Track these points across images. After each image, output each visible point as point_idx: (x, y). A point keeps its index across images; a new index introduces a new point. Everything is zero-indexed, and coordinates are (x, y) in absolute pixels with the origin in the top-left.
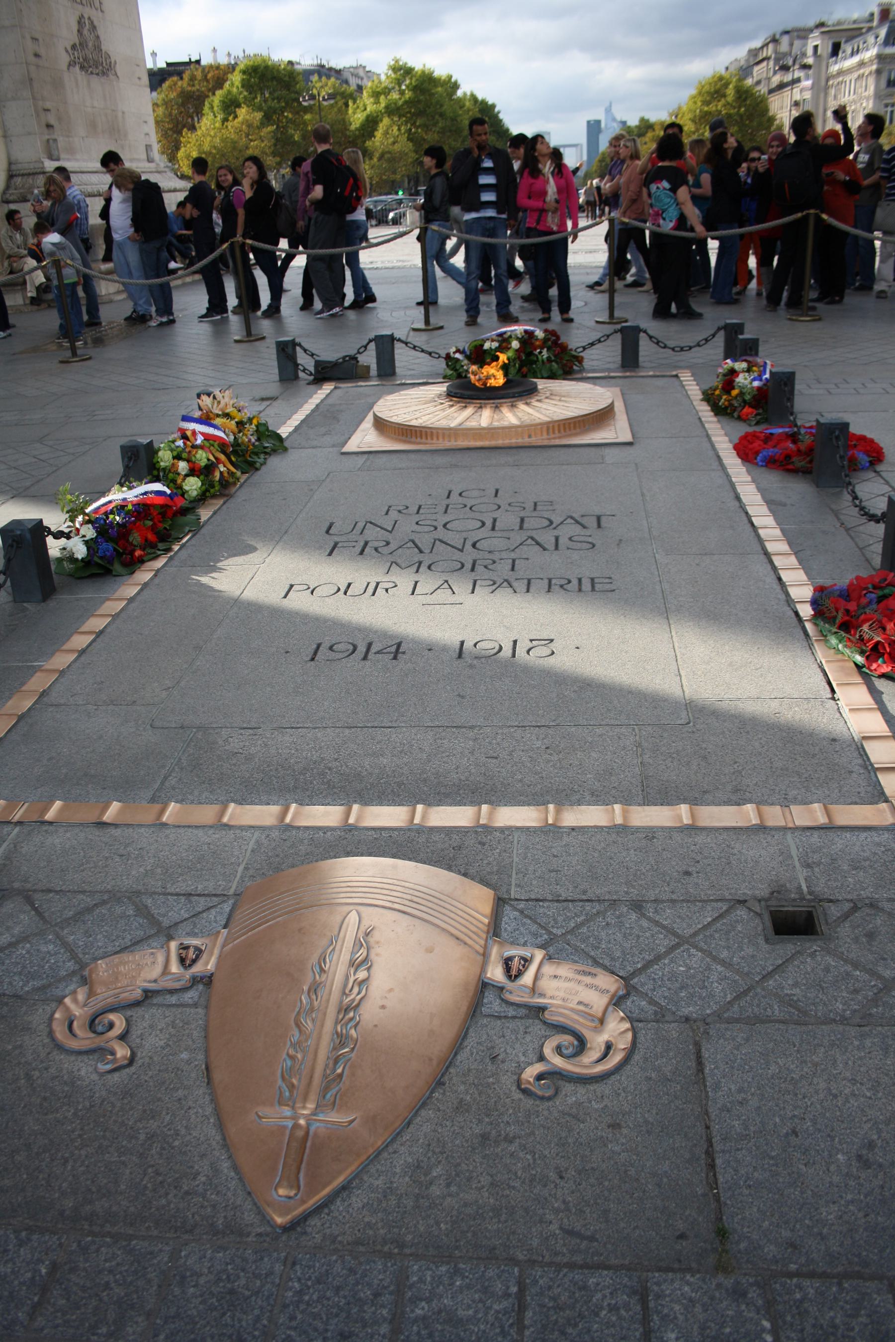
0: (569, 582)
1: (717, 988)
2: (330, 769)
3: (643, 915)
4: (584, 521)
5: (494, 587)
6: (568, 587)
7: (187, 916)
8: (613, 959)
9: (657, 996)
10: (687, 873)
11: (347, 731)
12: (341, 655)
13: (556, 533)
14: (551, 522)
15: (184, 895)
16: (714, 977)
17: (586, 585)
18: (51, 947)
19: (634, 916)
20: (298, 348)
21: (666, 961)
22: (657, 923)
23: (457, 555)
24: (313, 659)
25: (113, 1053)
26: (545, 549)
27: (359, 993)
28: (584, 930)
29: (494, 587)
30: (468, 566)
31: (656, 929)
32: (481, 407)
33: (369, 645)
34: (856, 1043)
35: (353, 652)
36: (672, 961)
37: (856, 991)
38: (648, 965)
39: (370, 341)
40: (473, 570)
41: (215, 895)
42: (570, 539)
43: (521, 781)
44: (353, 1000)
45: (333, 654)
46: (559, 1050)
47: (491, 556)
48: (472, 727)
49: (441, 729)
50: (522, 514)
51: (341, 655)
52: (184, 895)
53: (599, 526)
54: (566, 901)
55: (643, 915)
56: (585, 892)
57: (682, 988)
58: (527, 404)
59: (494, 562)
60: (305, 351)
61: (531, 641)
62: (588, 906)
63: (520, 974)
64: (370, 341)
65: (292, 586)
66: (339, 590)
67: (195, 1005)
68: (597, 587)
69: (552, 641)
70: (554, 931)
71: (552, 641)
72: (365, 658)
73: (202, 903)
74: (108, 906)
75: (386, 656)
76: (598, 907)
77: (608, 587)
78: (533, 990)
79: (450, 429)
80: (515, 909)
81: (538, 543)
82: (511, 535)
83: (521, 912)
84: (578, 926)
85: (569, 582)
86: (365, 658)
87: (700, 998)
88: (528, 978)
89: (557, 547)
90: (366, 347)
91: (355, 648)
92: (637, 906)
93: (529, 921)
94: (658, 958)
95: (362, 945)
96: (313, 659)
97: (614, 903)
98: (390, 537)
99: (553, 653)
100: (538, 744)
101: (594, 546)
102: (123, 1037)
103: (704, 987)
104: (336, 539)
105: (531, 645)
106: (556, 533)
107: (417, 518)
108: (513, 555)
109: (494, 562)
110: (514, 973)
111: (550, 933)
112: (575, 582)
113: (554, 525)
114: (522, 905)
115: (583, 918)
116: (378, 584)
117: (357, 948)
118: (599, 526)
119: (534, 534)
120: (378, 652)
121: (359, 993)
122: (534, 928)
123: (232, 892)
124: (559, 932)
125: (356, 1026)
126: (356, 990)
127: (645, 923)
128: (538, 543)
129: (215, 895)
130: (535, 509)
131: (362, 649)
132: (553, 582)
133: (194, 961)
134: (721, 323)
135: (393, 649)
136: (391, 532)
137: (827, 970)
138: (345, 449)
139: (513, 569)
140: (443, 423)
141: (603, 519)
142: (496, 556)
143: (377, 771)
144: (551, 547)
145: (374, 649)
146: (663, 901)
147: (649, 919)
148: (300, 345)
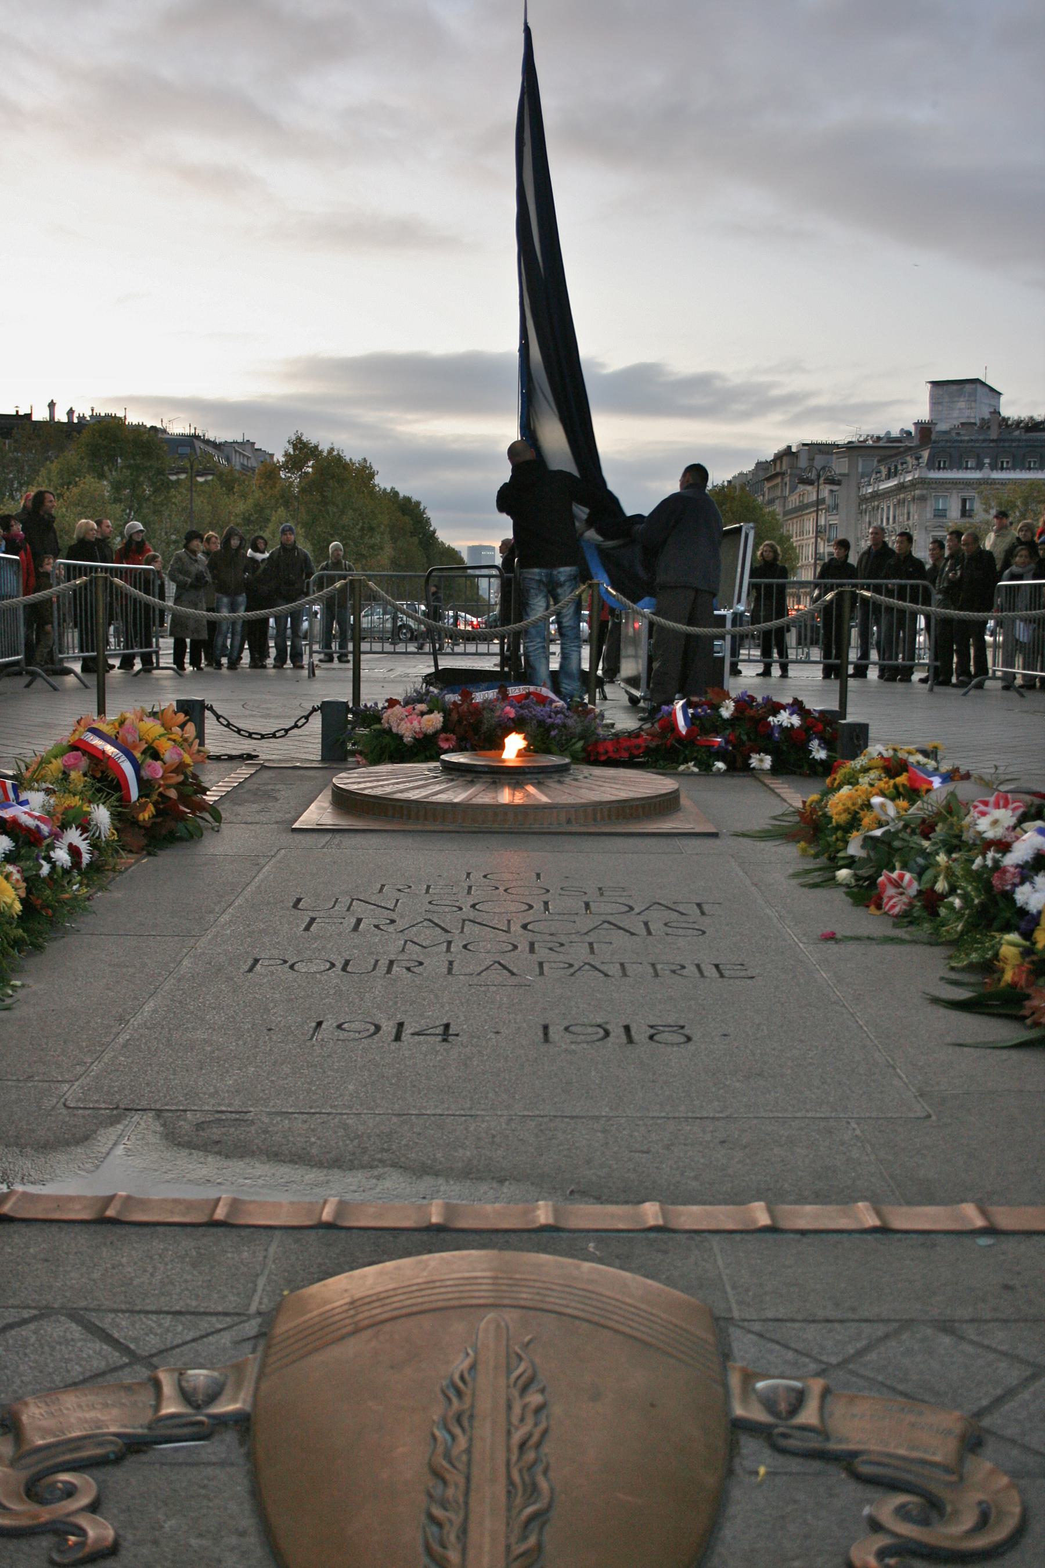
3: (962, 1338)
4: (681, 908)
5: (572, 970)
6: (685, 972)
7: (179, 1341)
10: (1007, 1287)
11: (395, 1119)
13: (642, 918)
14: (631, 908)
15: (168, 1313)
17: (710, 971)
19: (947, 1340)
20: (207, 713)
22: (988, 1348)
23: (503, 936)
25: (81, 1532)
27: (536, 1425)
28: (873, 1356)
29: (572, 970)
31: (991, 1356)
32: (494, 783)
35: (375, 1033)
38: (998, 1401)
39: (314, 710)
40: (532, 950)
41: (226, 1314)
43: (696, 1178)
44: (530, 1435)
45: (346, 1034)
46: (902, 1512)
47: (554, 939)
48: (596, 1118)
49: (546, 1120)
50: (586, 899)
52: (168, 1313)
53: (703, 913)
54: (828, 1321)
55: (962, 1338)
56: (853, 1309)
58: (560, 782)
59: (562, 945)
60: (218, 717)
61: (652, 1027)
62: (867, 1328)
63: (795, 1409)
64: (314, 710)
65: (256, 961)
67: (222, 1464)
68: (726, 973)
70: (824, 1358)
71: (682, 1027)
72: (398, 1038)
73: (205, 1324)
74: (32, 1326)
76: (881, 1330)
77: (743, 974)
78: (823, 1432)
79: (455, 805)
80: (750, 1332)
81: (620, 928)
82: (576, 918)
83: (761, 1336)
84: (860, 1353)
90: (307, 718)
91: (378, 1028)
92: (946, 1326)
93: (778, 1347)
95: (520, 1358)
97: (907, 1324)
98: (394, 916)
99: (689, 1039)
102: (94, 1508)
105: (653, 1031)
106: (642, 918)
107: (428, 898)
108: (588, 939)
109: (562, 945)
110: (783, 1406)
112: (691, 970)
113: (637, 910)
114: (757, 1327)
115: (864, 1342)
117: (514, 1361)
118: (703, 913)
119: (610, 918)
120: (413, 1034)
121: (536, 1425)
122: (790, 1355)
123: (253, 1309)
124: (834, 1360)
125: (545, 1472)
126: (530, 1421)
127: (970, 1349)
128: (620, 928)
129: (226, 1314)
130: (602, 895)
131: (388, 1028)
132: (659, 967)
136: (393, 910)
138: (296, 825)
140: (443, 798)
141: (706, 908)
142: (563, 939)
143: (460, 1165)
145: (408, 1031)
146: (987, 1321)
147: (972, 1342)
148: (211, 709)
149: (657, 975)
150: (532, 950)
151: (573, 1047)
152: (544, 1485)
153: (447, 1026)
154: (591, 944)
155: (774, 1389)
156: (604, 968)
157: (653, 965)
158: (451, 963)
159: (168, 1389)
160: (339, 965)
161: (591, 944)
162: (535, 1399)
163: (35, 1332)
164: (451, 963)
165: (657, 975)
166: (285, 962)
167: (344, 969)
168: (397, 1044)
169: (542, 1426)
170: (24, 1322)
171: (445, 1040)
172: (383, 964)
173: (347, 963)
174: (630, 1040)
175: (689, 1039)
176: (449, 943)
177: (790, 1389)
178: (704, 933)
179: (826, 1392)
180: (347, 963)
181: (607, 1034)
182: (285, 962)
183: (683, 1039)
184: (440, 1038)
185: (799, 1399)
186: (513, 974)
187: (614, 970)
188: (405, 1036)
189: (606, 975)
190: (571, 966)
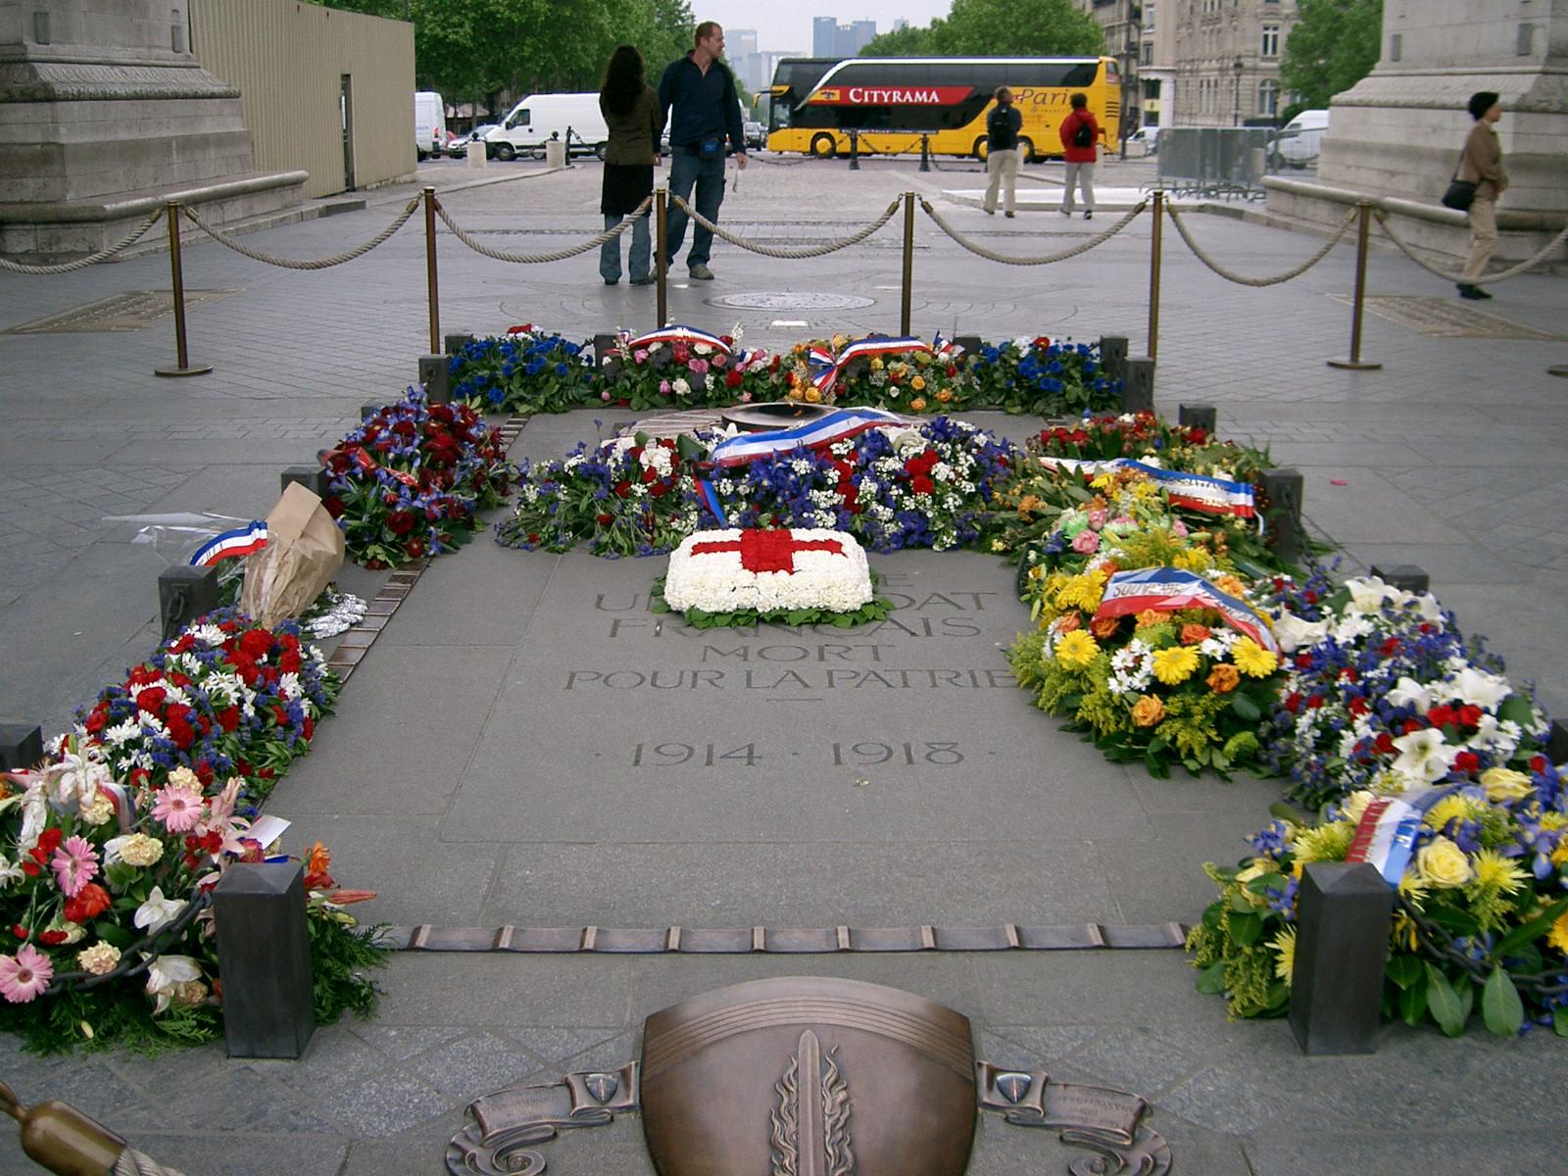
0: (958, 675)
1: (1256, 1106)
2: (708, 889)
8: (1126, 1081)
9: (1189, 1115)
12: (675, 760)
13: (922, 614)
14: (912, 601)
16: (1249, 1095)
18: (408, 1086)
19: (1141, 1039)
21: (1191, 1081)
22: (1170, 1045)
24: (637, 762)
26: (913, 634)
30: (814, 654)
33: (710, 749)
34: (1422, 1149)
35: (690, 755)
36: (1196, 1080)
37: (1412, 1103)
40: (822, 658)
42: (944, 621)
51: (675, 760)
53: (979, 607)
57: (1215, 1106)
61: (928, 745)
63: (1022, 1096)
65: (573, 676)
66: (643, 679)
68: (997, 681)
69: (955, 744)
70: (1049, 1055)
71: (955, 744)
72: (709, 763)
74: (467, 1040)
75: (738, 762)
83: (1003, 1037)
85: (958, 675)
86: (709, 763)
87: (1238, 1114)
88: (1033, 1101)
89: (929, 633)
91: (691, 750)
94: (1179, 1078)
96: (637, 762)
99: (961, 757)
100: (973, 861)
101: (979, 632)
103: (1239, 1105)
104: (616, 616)
106: (922, 614)
111: (1044, 1058)
112: (966, 676)
116: (695, 675)
118: (979, 607)
127: (1155, 1045)
131: (701, 751)
133: (611, 1095)
134: (1097, 339)
135: (745, 752)
137: (1377, 1084)
139: (877, 659)
144: (921, 631)
145: (718, 751)
149: (934, 685)
150: (822, 658)
151: (861, 768)
152: (847, 1152)
153: (751, 748)
154: (875, 649)
155: (1010, 1080)
156: (887, 677)
157: (932, 674)
158: (749, 674)
159: (579, 1091)
160: (649, 679)
161: (875, 649)
162: (842, 1096)
163: (470, 1045)
164: (749, 674)
165: (934, 685)
166: (600, 675)
167: (653, 684)
168: (709, 768)
169: (847, 1113)
170: (460, 1038)
171: (749, 764)
172: (688, 678)
173: (655, 675)
174: (910, 760)
175: (961, 757)
176: (746, 649)
177: (1019, 1080)
178: (979, 632)
179: (1047, 1081)
180: (655, 675)
181: (890, 752)
182: (600, 675)
183: (955, 758)
184: (745, 761)
185: (1027, 1087)
186: (806, 686)
187: (896, 679)
188: (715, 759)
189: (889, 686)
190: (857, 674)
